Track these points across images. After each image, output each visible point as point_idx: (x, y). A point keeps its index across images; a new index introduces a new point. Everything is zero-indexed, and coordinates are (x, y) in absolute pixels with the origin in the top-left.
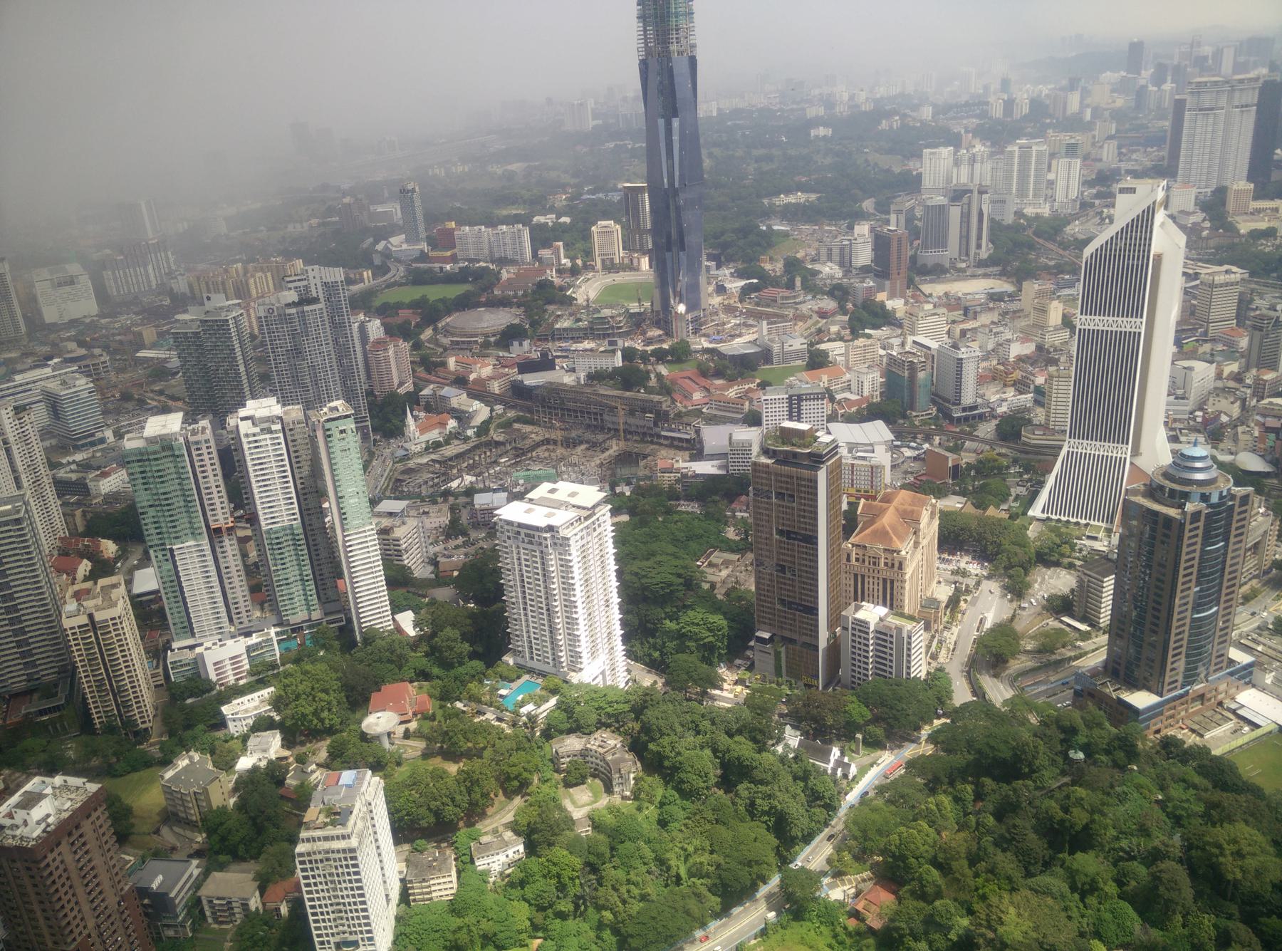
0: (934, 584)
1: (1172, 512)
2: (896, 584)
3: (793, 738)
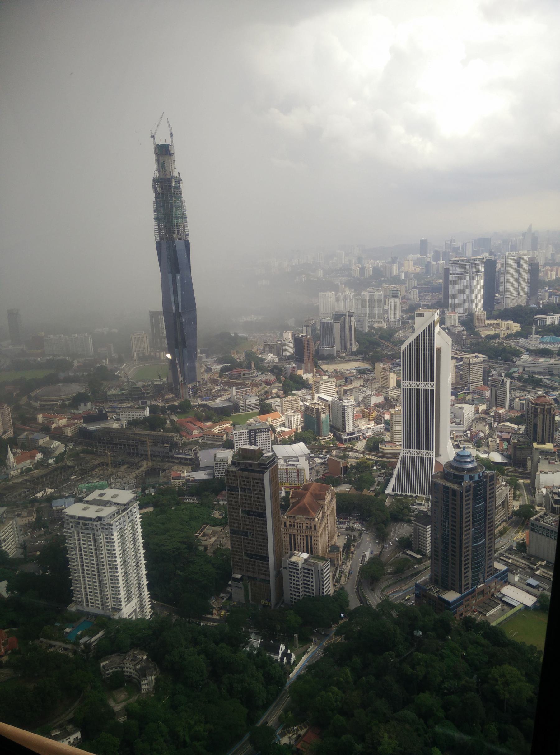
0: (336, 537)
1: (455, 487)
2: (313, 538)
3: (256, 642)
